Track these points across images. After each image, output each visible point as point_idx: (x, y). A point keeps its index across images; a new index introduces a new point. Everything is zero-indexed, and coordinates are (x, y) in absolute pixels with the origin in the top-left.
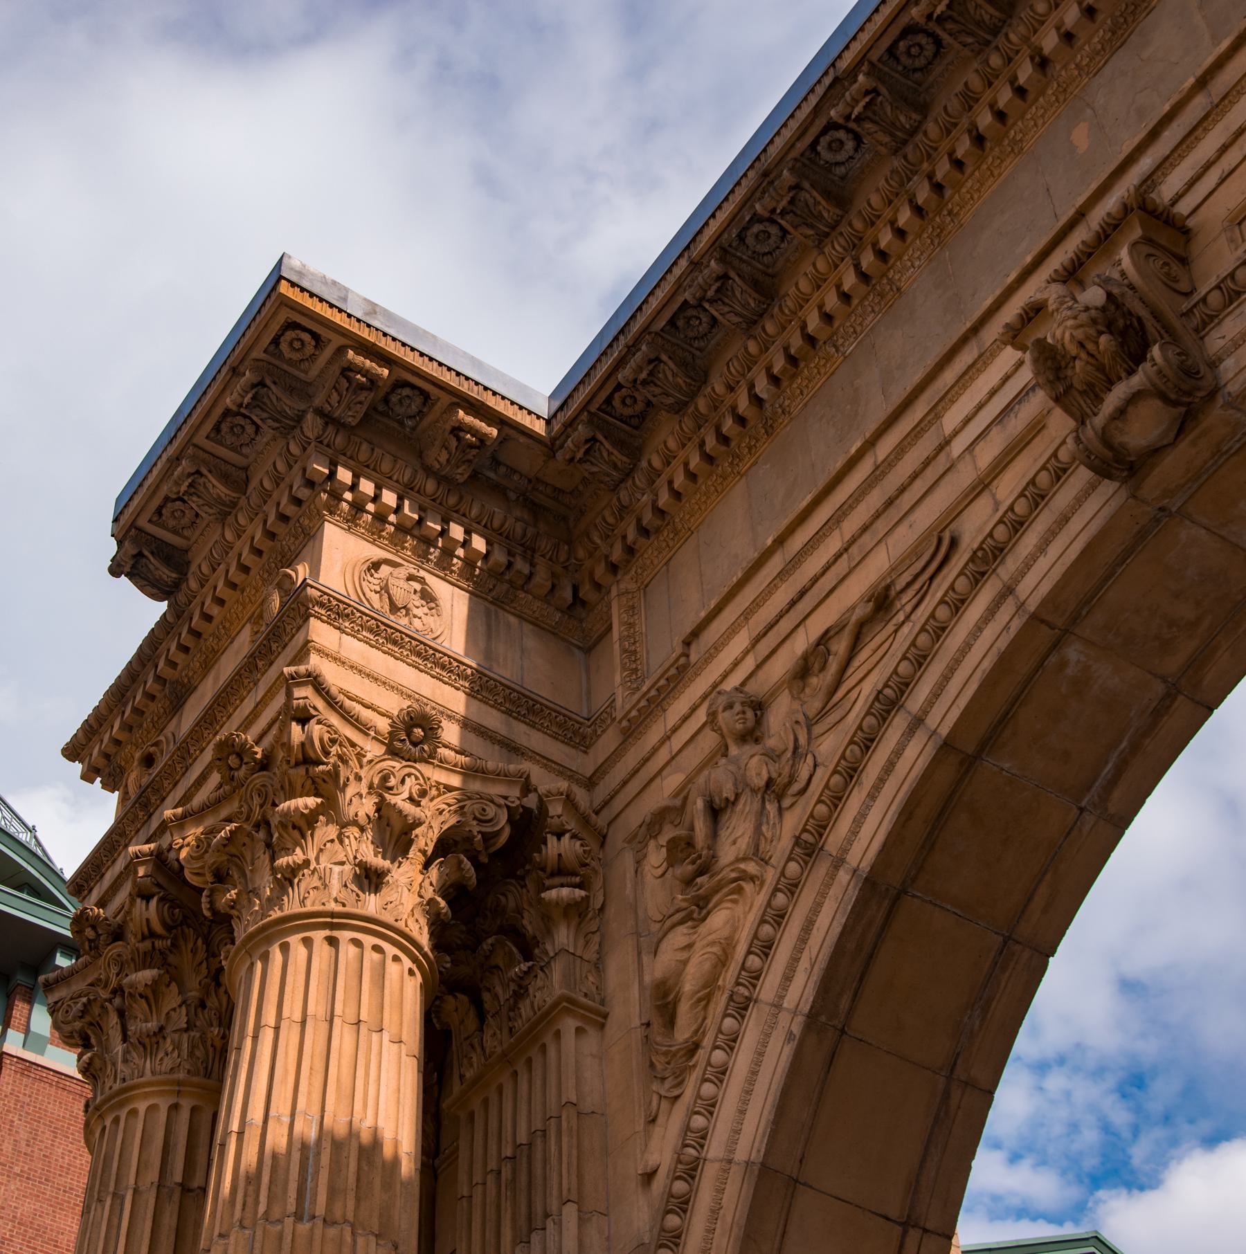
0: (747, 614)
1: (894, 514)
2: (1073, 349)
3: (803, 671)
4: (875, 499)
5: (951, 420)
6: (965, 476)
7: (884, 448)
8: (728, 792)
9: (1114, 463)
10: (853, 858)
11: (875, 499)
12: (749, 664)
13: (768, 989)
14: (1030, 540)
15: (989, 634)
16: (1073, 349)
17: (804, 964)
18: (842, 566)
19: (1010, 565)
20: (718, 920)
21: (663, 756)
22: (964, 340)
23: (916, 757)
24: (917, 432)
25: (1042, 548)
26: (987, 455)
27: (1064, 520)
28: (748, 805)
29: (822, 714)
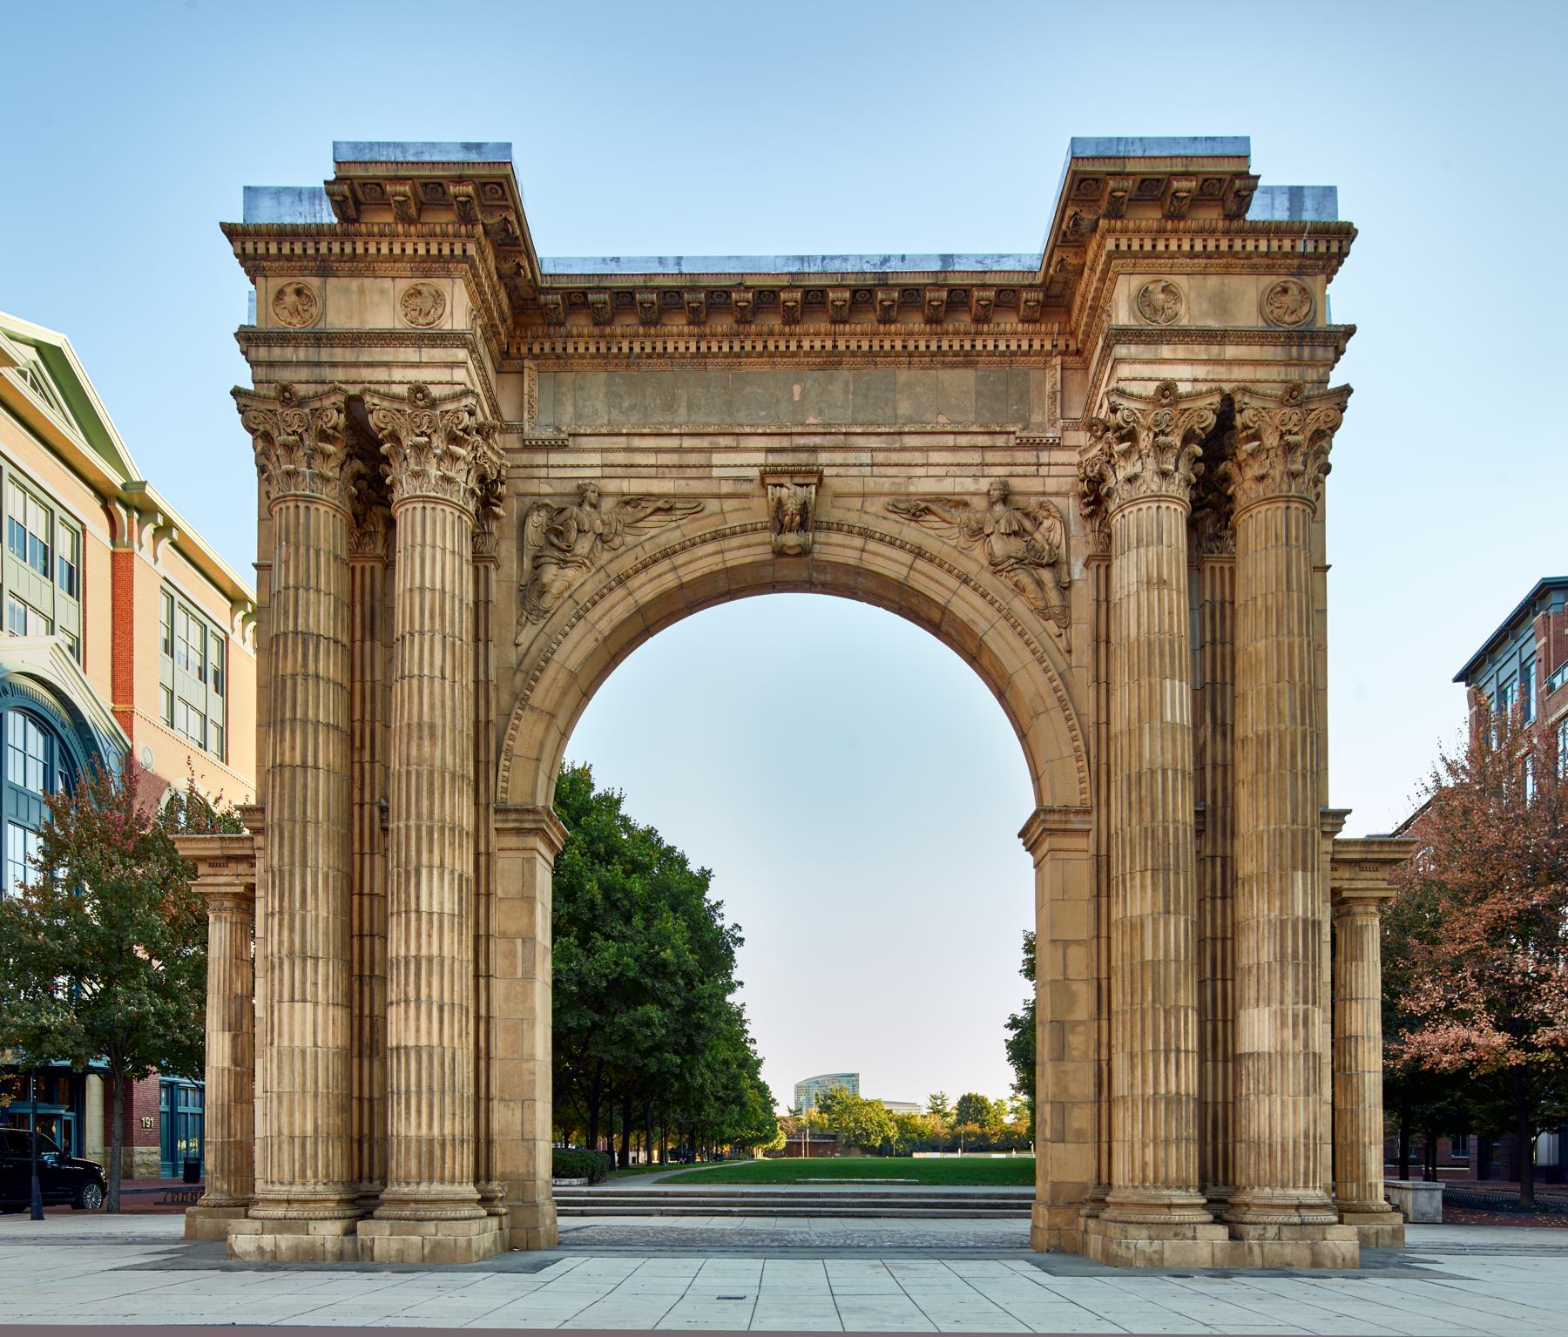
0: (603, 450)
1: (681, 472)
3: (629, 501)
4: (672, 459)
5: (717, 458)
6: (712, 487)
7: (688, 443)
8: (586, 527)
9: (780, 552)
10: (638, 595)
11: (672, 459)
12: (597, 472)
13: (593, 615)
14: (735, 542)
15: (710, 560)
17: (607, 618)
18: (653, 471)
19: (725, 544)
20: (570, 573)
21: (543, 472)
23: (670, 581)
24: (701, 450)
25: (740, 548)
26: (726, 488)
27: (749, 546)
28: (591, 536)
29: (629, 525)
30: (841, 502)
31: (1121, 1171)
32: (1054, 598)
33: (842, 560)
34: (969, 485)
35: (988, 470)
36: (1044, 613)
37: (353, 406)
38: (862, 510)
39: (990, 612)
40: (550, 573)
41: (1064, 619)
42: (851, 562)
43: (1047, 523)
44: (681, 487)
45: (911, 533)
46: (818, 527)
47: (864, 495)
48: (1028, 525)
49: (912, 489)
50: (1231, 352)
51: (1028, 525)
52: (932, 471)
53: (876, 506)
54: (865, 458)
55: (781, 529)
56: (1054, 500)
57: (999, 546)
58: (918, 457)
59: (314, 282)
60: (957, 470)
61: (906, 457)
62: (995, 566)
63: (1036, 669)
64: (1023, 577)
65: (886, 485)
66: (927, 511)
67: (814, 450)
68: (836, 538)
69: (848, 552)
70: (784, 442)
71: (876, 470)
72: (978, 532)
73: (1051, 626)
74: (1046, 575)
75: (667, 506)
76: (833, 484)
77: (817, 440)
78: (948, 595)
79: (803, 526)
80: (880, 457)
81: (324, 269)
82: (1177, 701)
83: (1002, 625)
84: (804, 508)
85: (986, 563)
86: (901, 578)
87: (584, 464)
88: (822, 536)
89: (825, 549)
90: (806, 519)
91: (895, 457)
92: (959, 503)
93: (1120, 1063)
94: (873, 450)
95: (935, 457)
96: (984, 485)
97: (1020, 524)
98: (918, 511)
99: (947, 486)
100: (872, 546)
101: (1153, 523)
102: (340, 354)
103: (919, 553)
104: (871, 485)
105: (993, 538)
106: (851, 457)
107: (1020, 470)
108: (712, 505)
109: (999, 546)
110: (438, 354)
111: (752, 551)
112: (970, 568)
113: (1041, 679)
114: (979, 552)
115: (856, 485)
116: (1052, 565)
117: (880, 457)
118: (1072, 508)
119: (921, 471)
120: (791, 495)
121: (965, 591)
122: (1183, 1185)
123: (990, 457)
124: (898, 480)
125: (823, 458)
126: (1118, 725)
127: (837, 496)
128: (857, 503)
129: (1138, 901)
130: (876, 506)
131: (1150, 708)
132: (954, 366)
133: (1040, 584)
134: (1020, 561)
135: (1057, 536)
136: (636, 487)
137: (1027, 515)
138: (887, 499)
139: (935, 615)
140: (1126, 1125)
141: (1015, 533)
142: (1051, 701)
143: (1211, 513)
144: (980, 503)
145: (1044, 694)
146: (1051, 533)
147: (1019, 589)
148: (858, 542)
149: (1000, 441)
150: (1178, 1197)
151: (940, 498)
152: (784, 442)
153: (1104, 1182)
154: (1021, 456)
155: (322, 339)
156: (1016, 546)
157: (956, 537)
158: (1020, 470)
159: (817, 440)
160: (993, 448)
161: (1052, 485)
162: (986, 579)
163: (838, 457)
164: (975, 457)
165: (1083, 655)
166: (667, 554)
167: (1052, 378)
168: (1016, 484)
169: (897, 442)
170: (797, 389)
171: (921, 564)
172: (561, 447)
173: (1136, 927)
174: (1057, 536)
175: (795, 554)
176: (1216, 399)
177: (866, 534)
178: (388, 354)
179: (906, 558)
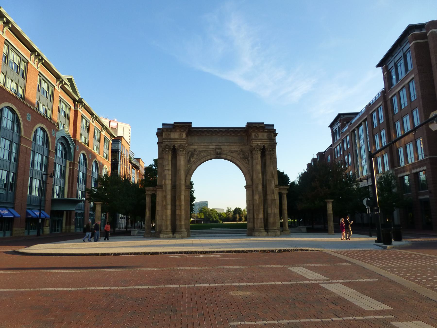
3: (201, 151)
31: (256, 226)
34: (237, 149)
36: (246, 163)
37: (174, 146)
40: (192, 159)
41: (248, 164)
44: (206, 149)
45: (231, 154)
53: (227, 151)
57: (241, 156)
59: (169, 133)
62: (241, 158)
72: (239, 154)
75: (204, 151)
81: (171, 132)
82: (260, 176)
84: (220, 152)
87: (195, 147)
90: (220, 154)
93: (255, 214)
99: (235, 149)
101: (258, 157)
102: (172, 140)
103: (232, 157)
108: (209, 151)
109: (241, 156)
110: (183, 140)
114: (239, 156)
116: (247, 158)
118: (249, 152)
122: (262, 227)
126: (254, 178)
129: (256, 197)
130: (227, 151)
131: (257, 177)
135: (247, 155)
136: (201, 149)
140: (256, 221)
143: (263, 155)
146: (247, 154)
150: (261, 229)
153: (254, 227)
155: (170, 139)
157: (236, 155)
165: (251, 168)
166: (205, 157)
167: (247, 138)
172: (193, 145)
173: (256, 200)
174: (247, 155)
175: (218, 155)
178: (177, 140)
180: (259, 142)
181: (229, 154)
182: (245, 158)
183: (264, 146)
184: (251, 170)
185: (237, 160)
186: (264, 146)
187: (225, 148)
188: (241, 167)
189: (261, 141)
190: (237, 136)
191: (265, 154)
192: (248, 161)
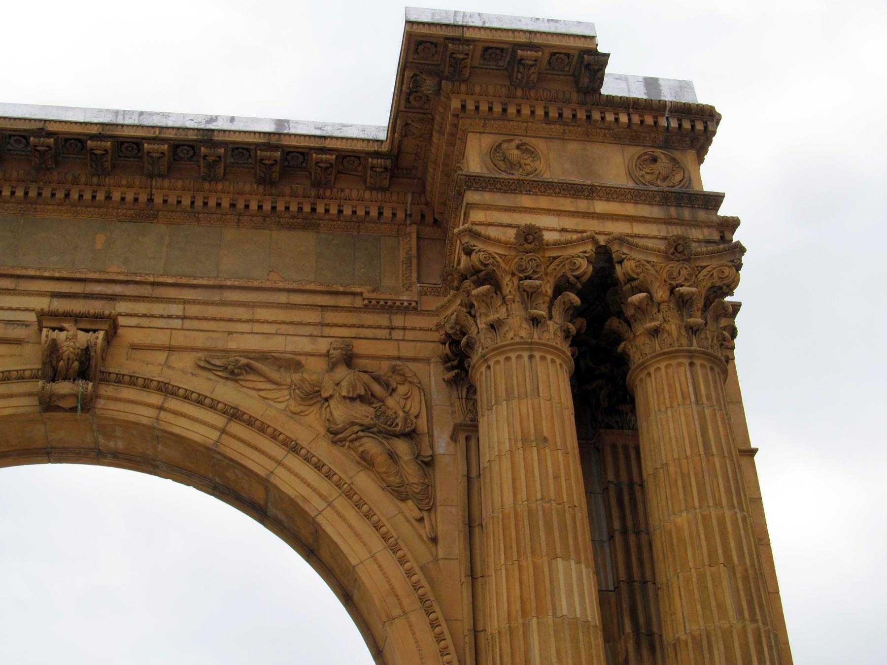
2: (65, 358)
9: (48, 404)
16: (65, 358)
22: (13, 276)
27: (11, 396)
30: (139, 355)
32: (412, 474)
33: (132, 418)
34: (305, 344)
35: (327, 331)
36: (399, 493)
38: (167, 364)
39: (324, 486)
41: (426, 501)
42: (144, 421)
43: (402, 389)
45: (227, 393)
46: (105, 378)
47: (170, 349)
48: (377, 389)
49: (232, 345)
50: (601, 207)
51: (377, 389)
52: (257, 328)
53: (186, 361)
54: (175, 309)
55: (55, 377)
56: (411, 365)
57: (340, 412)
58: (243, 313)
60: (291, 329)
61: (228, 312)
62: (335, 435)
63: (388, 560)
64: (371, 446)
65: (200, 340)
66: (249, 369)
67: (113, 298)
68: (127, 393)
69: (141, 410)
70: (77, 288)
71: (188, 324)
72: (313, 396)
73: (410, 508)
74: (402, 447)
76: (129, 335)
77: (118, 289)
78: (271, 465)
79: (83, 374)
80: (194, 310)
83: (342, 504)
85: (322, 431)
86: (209, 443)
88: (107, 390)
89: (112, 405)
90: (85, 367)
91: (212, 311)
92: (292, 364)
94: (185, 302)
95: (263, 314)
96: (323, 345)
97: (367, 387)
98: (237, 370)
99: (276, 344)
100: (173, 404)
103: (234, 414)
104: (180, 339)
105: (333, 403)
106: (158, 309)
107: (368, 333)
109: (340, 412)
111: (14, 402)
112: (301, 434)
113: (396, 574)
114: (314, 418)
115: (162, 338)
116: (410, 435)
117: (194, 310)
118: (434, 376)
119: (245, 327)
120: (73, 339)
121: (292, 461)
123: (331, 317)
124: (214, 335)
125: (122, 307)
127: (135, 347)
128: (161, 357)
130: (186, 361)
132: (291, 227)
133: (392, 456)
134: (366, 429)
135: (415, 405)
137: (377, 379)
138: (200, 355)
139: (259, 495)
141: (361, 399)
142: (410, 601)
144: (316, 366)
145: (400, 592)
147: (367, 462)
148: (155, 399)
149: (345, 301)
151: (264, 356)
152: (77, 288)
154: (369, 319)
156: (363, 413)
158: (368, 333)
159: (118, 289)
160: (335, 308)
161: (407, 350)
162: (323, 450)
163: (141, 308)
164: (313, 317)
165: (452, 543)
168: (360, 347)
169: (216, 296)
170: (101, 239)
171: (236, 428)
176: (589, 248)
177: (166, 389)
179: (218, 420)
180: (545, 210)
181: (201, 384)
182: (382, 432)
183: (605, 258)
184: (454, 571)
185: (294, 448)
186: (605, 258)
187: (161, 338)
188: (340, 527)
189: (567, 204)
190: (307, 222)
191: (623, 361)
192: (428, 464)
